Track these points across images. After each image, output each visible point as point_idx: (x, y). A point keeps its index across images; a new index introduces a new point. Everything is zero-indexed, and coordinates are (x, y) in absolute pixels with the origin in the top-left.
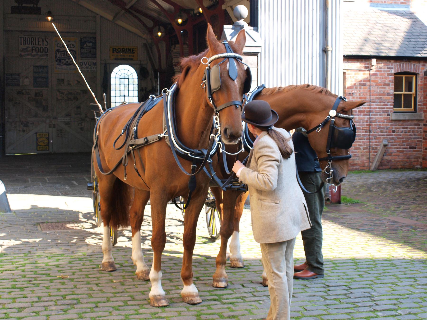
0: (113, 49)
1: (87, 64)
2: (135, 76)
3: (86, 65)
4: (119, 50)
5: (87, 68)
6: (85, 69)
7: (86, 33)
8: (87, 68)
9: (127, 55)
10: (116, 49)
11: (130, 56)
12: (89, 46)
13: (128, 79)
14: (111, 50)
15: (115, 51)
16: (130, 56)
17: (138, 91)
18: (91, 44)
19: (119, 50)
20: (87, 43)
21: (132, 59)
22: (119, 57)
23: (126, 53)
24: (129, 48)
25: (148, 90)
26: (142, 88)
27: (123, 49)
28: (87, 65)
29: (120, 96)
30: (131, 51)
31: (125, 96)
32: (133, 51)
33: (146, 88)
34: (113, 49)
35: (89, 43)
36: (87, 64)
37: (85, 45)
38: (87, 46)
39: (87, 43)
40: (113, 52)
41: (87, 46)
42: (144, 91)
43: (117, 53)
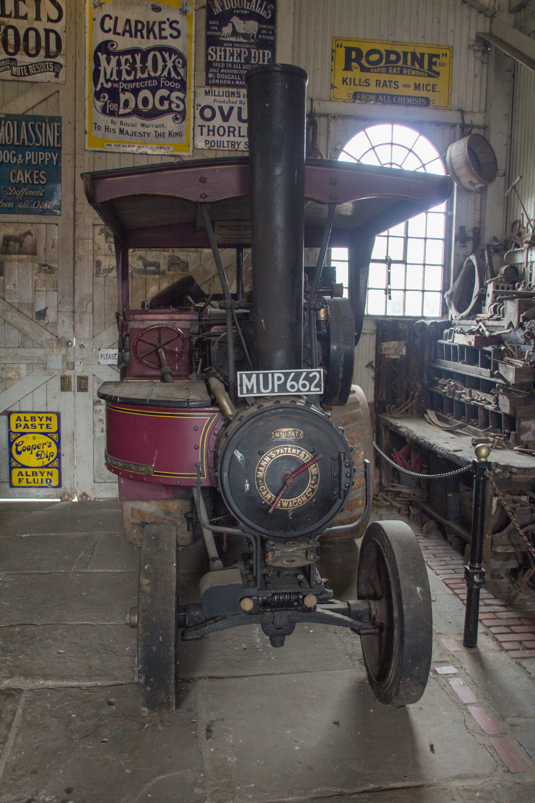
0: (349, 50)
1: (235, 112)
3: (226, 119)
4: (374, 57)
5: (231, 131)
6: (225, 138)
8: (231, 131)
10: (359, 52)
12: (245, 36)
14: (341, 53)
15: (358, 60)
16: (417, 87)
17: (447, 241)
18: (252, 27)
19: (374, 57)
20: (235, 20)
22: (373, 89)
23: (401, 73)
24: (418, 51)
27: (389, 53)
28: (234, 121)
30: (426, 64)
34: (349, 50)
35: (242, 17)
36: (235, 112)
37: (227, 30)
38: (235, 33)
39: (235, 20)
40: (348, 67)
41: (235, 33)
43: (363, 69)
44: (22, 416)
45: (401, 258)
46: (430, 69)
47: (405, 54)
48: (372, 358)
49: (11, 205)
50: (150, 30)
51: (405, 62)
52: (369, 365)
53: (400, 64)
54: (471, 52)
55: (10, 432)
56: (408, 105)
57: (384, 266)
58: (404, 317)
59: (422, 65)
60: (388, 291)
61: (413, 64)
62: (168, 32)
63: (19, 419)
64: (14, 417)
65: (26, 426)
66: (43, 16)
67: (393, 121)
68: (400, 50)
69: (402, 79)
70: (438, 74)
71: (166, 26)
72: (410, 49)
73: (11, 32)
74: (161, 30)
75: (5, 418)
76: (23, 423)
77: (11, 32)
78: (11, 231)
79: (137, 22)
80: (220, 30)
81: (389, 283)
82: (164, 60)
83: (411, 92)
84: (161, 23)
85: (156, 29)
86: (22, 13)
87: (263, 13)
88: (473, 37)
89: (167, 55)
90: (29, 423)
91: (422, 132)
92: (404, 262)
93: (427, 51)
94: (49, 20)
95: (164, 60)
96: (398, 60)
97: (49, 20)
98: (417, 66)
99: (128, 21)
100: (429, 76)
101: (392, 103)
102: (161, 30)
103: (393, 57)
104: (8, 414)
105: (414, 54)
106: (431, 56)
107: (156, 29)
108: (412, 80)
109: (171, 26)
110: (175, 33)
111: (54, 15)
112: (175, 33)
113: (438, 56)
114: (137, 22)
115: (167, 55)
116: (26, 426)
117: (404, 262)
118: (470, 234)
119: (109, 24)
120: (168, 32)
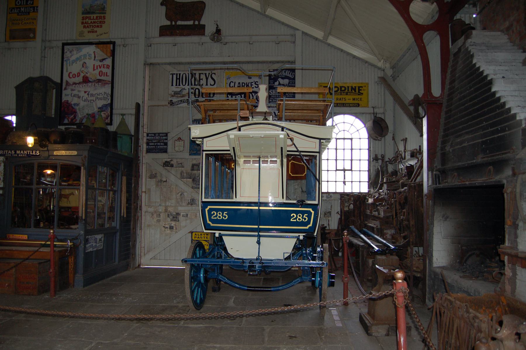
2: (364, 133)
7: (278, 62)
9: (349, 98)
11: (354, 99)
13: (351, 139)
16: (354, 99)
17: (369, 160)
20: (280, 79)
21: (358, 105)
23: (347, 94)
25: (387, 159)
26: (376, 155)
27: (341, 87)
29: (337, 170)
30: (357, 90)
31: (344, 170)
32: (359, 90)
33: (383, 157)
35: (283, 78)
37: (277, 83)
38: (280, 84)
39: (280, 79)
42: (380, 162)
44: (197, 233)
45: (350, 169)
46: (359, 92)
47: (348, 87)
48: (339, 210)
49: (195, 152)
50: (247, 86)
51: (348, 90)
52: (338, 213)
53: (346, 91)
54: (376, 84)
55: (192, 240)
56: (350, 107)
57: (343, 172)
58: (352, 193)
59: (355, 91)
60: (344, 183)
61: (352, 91)
62: (254, 85)
63: (196, 234)
64: (194, 234)
65: (199, 238)
66: (209, 84)
67: (344, 114)
68: (346, 86)
69: (347, 97)
70: (362, 94)
71: (253, 84)
72: (350, 85)
73: (197, 90)
74: (251, 85)
75: (190, 234)
76: (197, 236)
77: (197, 90)
78: (194, 162)
79: (242, 83)
80: (274, 83)
81: (345, 179)
82: (253, 96)
83: (351, 101)
84: (251, 83)
85: (250, 85)
86: (201, 84)
87: (290, 76)
88: (377, 79)
89: (254, 94)
90: (200, 236)
91: (357, 117)
92: (351, 170)
93: (357, 85)
94: (211, 85)
95: (253, 96)
96: (345, 90)
97: (211, 85)
98: (353, 91)
99: (239, 83)
100: (359, 95)
101: (344, 106)
102: (251, 85)
103: (343, 89)
104: (192, 233)
105: (352, 87)
106: (359, 87)
107: (250, 85)
108: (351, 97)
109: (255, 84)
110: (257, 86)
111: (213, 83)
112: (257, 86)
113: (362, 87)
114: (242, 83)
115: (254, 94)
116: (199, 238)
117: (351, 170)
118: (380, 157)
119: (232, 84)
120: (254, 85)
